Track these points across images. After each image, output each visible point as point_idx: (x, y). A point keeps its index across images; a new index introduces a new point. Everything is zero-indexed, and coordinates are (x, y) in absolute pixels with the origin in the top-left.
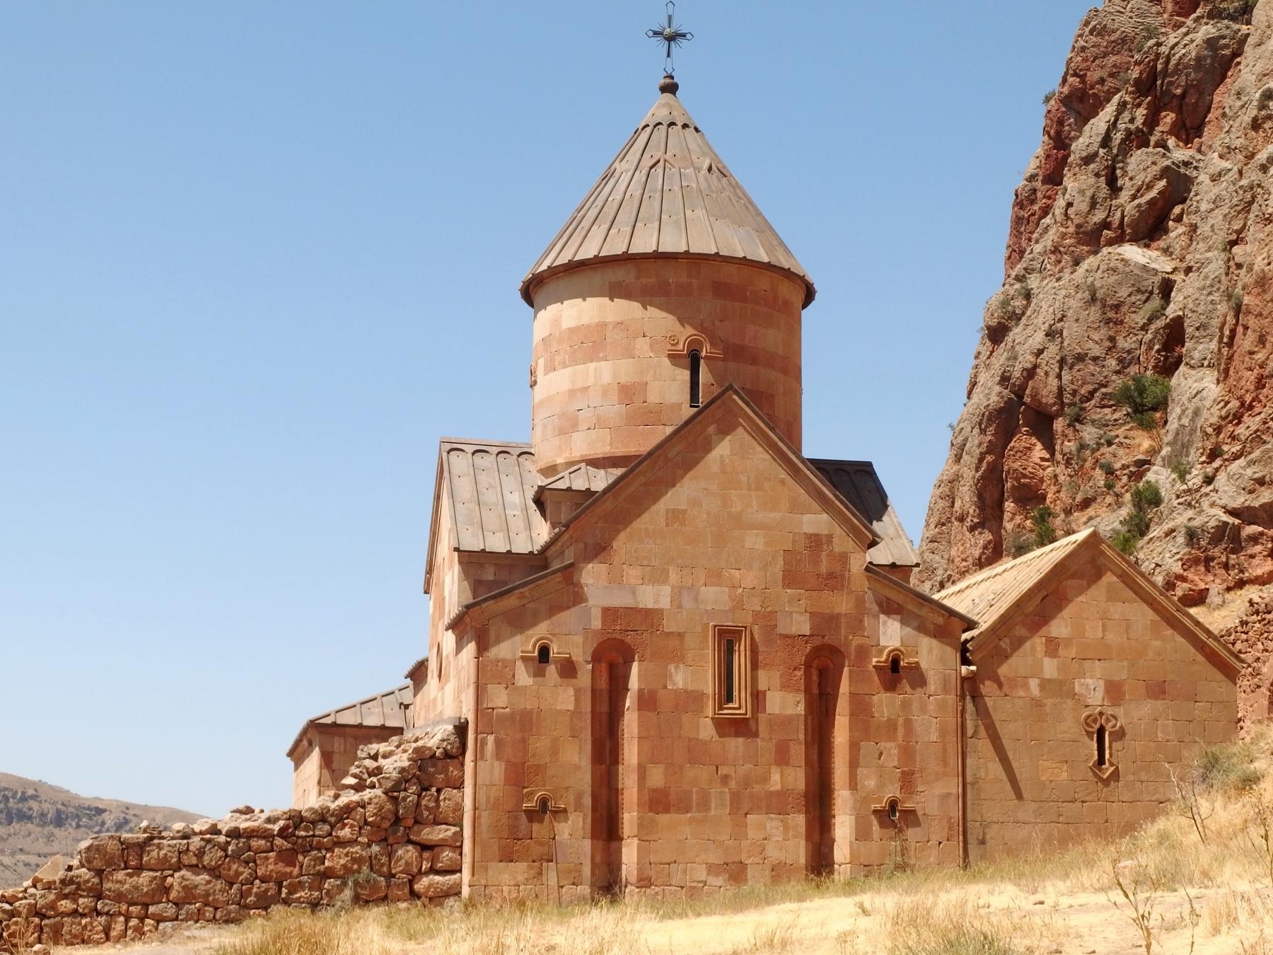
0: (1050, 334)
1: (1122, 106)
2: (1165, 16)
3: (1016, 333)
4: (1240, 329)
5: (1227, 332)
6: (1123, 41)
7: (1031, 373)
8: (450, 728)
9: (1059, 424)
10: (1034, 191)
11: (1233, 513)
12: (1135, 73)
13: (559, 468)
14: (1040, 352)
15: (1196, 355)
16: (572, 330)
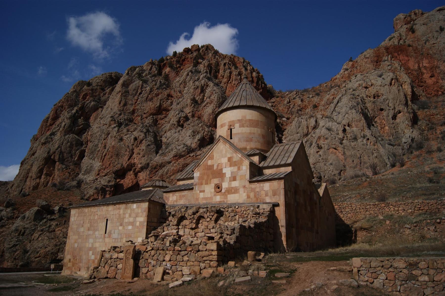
0: (59, 147)
1: (77, 110)
2: (80, 98)
3: (49, 145)
4: (107, 154)
5: (104, 154)
6: (73, 99)
7: (54, 153)
8: (272, 205)
9: (57, 163)
10: (48, 120)
11: (104, 185)
12: (80, 106)
13: (248, 149)
14: (57, 149)
15: (91, 157)
16: (250, 120)
